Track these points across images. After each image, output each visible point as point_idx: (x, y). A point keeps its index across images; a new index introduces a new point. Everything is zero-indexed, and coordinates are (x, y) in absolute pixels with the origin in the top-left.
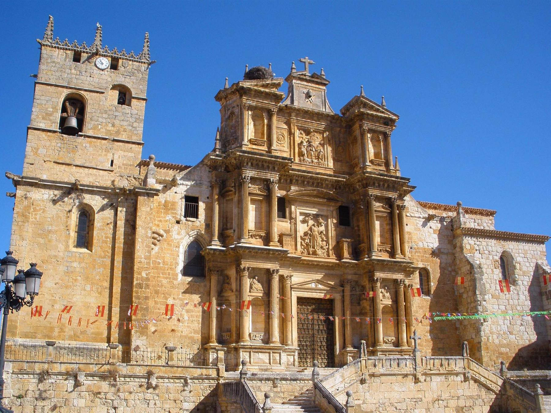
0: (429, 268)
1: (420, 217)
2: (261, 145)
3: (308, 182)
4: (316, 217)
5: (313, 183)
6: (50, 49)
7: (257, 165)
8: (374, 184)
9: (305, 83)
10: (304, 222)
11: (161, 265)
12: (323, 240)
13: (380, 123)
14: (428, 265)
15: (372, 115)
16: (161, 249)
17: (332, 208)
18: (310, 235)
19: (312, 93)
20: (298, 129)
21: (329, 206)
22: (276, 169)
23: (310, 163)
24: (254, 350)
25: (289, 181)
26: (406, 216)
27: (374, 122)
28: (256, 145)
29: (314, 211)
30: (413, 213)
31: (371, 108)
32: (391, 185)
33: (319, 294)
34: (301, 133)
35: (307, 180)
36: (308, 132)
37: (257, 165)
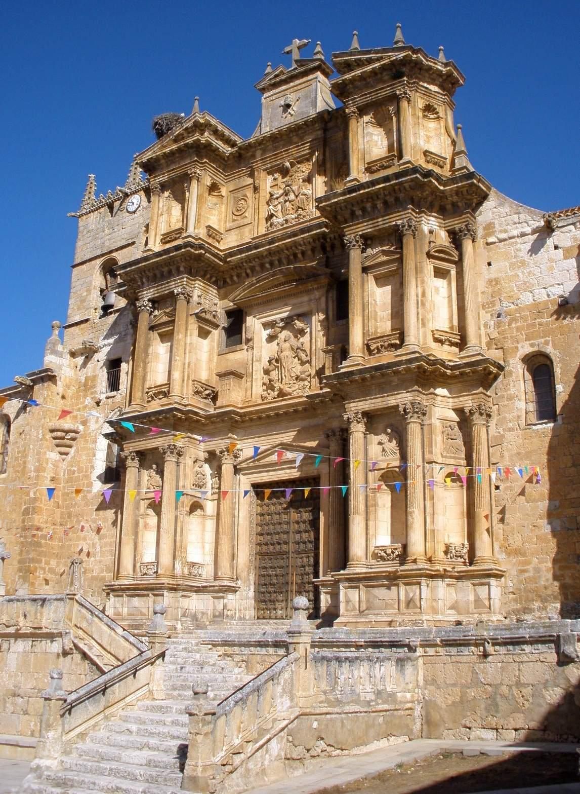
0: (549, 350)
1: (523, 235)
2: (176, 239)
3: (272, 264)
4: (288, 323)
5: (280, 261)
6: (86, 216)
7: (155, 275)
8: (353, 213)
9: (284, 87)
10: (271, 338)
11: (76, 474)
12: (303, 363)
13: (384, 82)
14: (547, 343)
15: (362, 77)
16: (77, 451)
17: (317, 294)
18: (277, 361)
19: (291, 98)
20: (269, 174)
21: (308, 292)
22: (182, 269)
23: (282, 225)
24: (128, 593)
25: (244, 275)
26: (488, 244)
27: (372, 87)
28: (169, 242)
29: (283, 313)
30: (506, 231)
31: (359, 64)
32: (391, 200)
33: (288, 471)
34: (275, 179)
35: (267, 260)
36: (285, 172)
37: (155, 275)
